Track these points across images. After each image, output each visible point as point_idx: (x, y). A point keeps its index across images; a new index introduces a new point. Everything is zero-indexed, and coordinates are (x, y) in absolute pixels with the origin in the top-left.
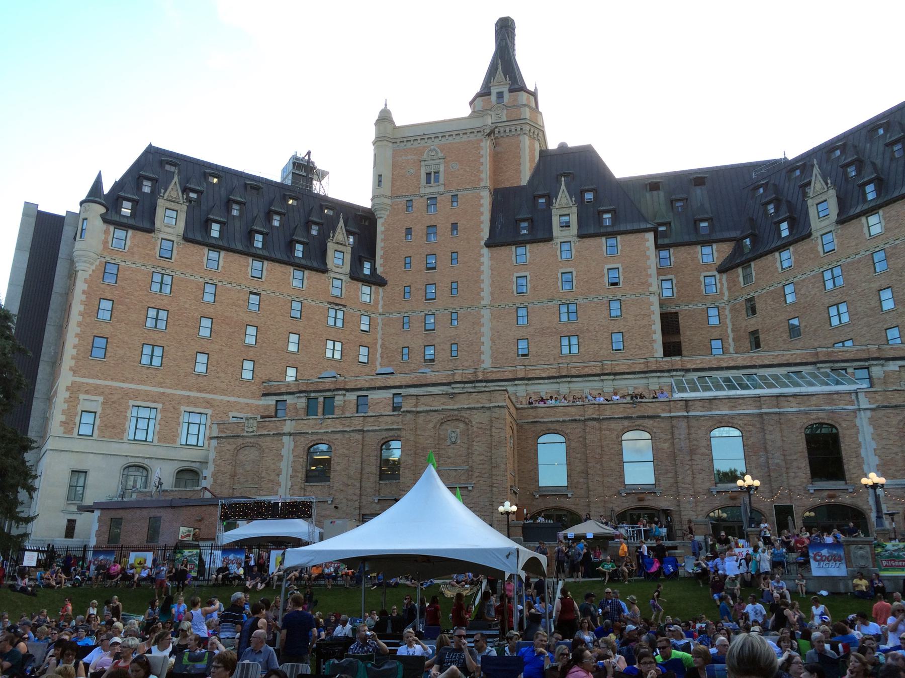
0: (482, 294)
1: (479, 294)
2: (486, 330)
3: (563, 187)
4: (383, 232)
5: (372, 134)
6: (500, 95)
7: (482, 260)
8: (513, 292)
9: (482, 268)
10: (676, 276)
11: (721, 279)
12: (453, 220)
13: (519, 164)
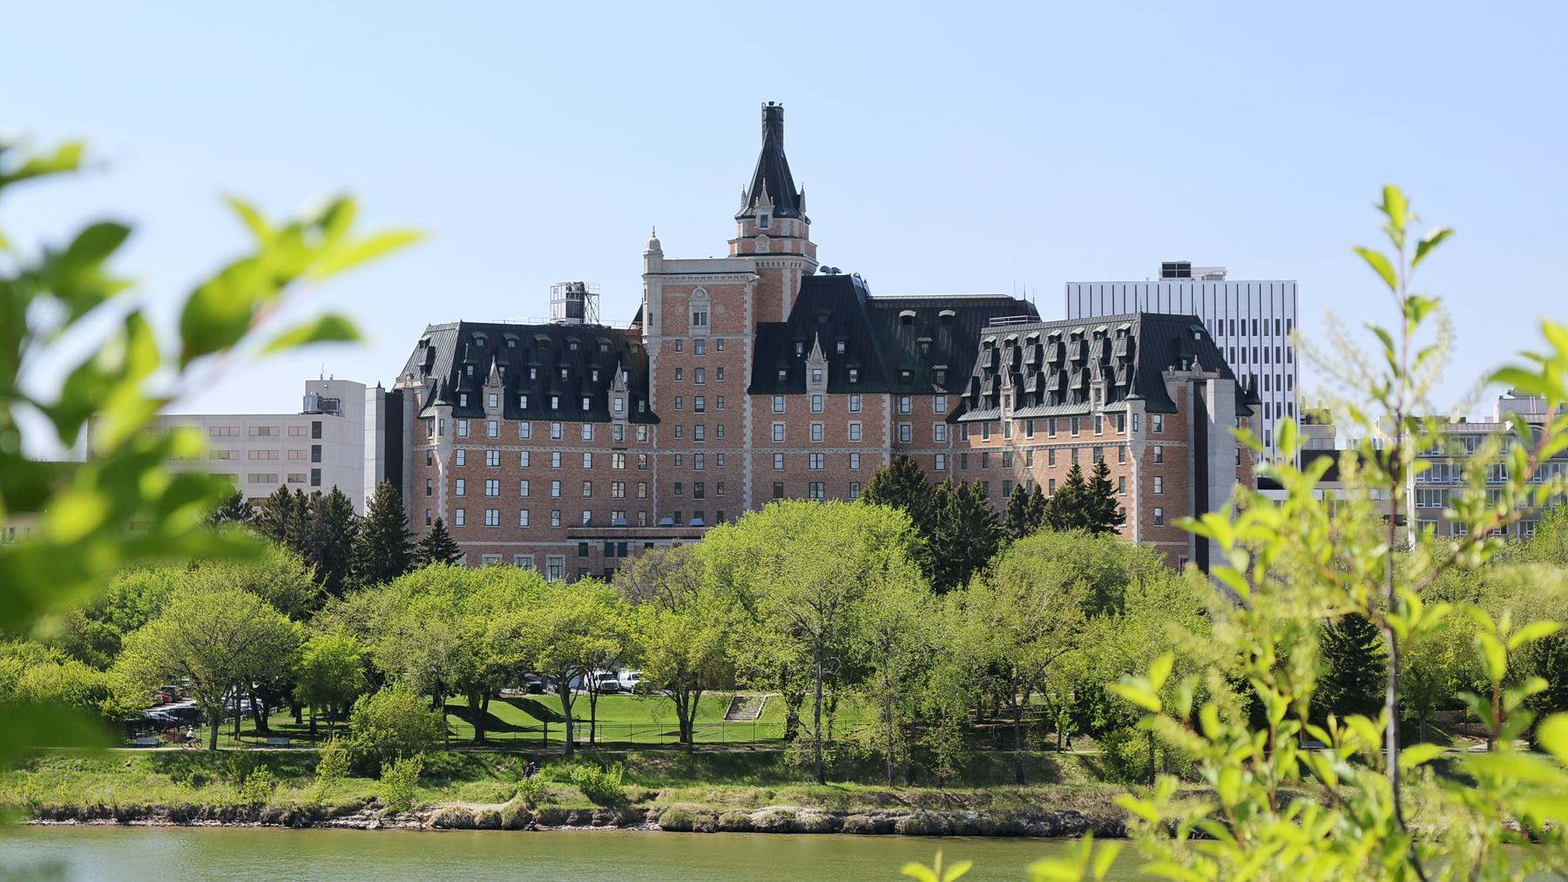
0: (745, 439)
1: (742, 438)
2: (748, 472)
3: (817, 343)
4: (655, 370)
5: (642, 267)
6: (764, 218)
7: (745, 406)
8: (771, 439)
9: (745, 414)
10: (913, 423)
11: (948, 429)
12: (719, 364)
13: (781, 300)
